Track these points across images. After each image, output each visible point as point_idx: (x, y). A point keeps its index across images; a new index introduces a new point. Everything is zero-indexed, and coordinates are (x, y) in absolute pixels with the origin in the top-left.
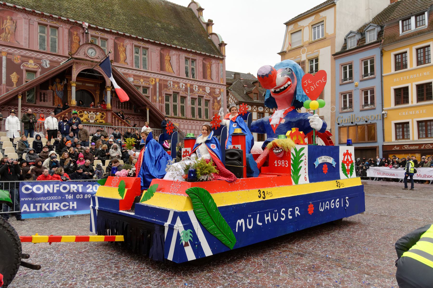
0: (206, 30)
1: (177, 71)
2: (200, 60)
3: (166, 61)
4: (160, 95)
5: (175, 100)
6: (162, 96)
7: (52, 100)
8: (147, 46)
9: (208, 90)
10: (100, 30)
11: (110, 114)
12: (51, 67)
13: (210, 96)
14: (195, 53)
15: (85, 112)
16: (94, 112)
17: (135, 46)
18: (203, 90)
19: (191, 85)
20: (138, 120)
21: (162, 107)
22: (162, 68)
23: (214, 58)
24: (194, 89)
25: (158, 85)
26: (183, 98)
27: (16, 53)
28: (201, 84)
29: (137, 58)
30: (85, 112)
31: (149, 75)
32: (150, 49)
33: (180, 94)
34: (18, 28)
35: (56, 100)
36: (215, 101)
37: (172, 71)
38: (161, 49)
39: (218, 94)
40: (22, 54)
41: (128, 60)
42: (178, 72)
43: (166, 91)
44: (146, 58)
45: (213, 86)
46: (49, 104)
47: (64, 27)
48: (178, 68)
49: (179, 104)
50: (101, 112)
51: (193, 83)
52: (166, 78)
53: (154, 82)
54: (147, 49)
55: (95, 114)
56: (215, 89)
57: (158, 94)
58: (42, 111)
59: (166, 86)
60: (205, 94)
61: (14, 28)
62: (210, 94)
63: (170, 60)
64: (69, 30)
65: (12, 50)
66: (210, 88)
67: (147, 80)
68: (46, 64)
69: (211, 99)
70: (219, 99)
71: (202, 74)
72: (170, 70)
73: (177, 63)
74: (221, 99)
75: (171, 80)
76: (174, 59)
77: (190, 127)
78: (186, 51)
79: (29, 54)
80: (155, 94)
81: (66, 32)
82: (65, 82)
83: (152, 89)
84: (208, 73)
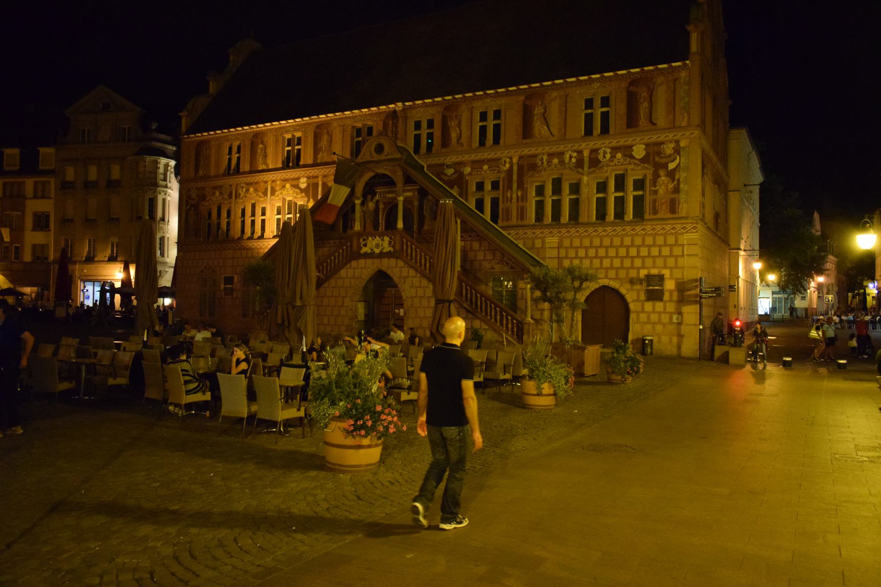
3: (535, 118)
4: (521, 186)
9: (639, 152)
13: (646, 165)
15: (370, 238)
16: (380, 237)
18: (624, 156)
19: (594, 151)
20: (479, 240)
24: (600, 157)
25: (515, 168)
29: (483, 130)
30: (370, 238)
39: (670, 155)
41: (464, 140)
42: (563, 130)
50: (388, 236)
53: (508, 166)
55: (381, 240)
57: (515, 185)
59: (533, 167)
60: (630, 164)
62: (644, 160)
63: (544, 114)
64: (384, 121)
66: (647, 145)
69: (649, 172)
70: (671, 166)
71: (625, 118)
72: (543, 132)
80: (510, 187)
83: (503, 178)
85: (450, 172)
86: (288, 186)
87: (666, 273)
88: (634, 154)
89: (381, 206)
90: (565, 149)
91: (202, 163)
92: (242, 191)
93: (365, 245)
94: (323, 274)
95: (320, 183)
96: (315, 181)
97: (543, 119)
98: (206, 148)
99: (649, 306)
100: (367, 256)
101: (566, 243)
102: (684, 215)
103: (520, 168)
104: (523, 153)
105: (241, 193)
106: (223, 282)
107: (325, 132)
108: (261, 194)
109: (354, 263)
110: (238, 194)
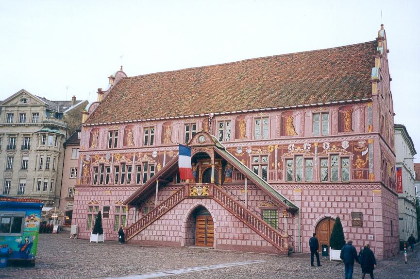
1: (301, 132)
2: (334, 111)
4: (279, 160)
6: (281, 163)
8: (267, 115)
9: (345, 145)
18: (337, 147)
21: (281, 173)
24: (324, 147)
25: (276, 151)
31: (267, 143)
32: (269, 117)
34: (173, 134)
38: (283, 113)
39: (363, 148)
41: (248, 135)
42: (303, 132)
43: (286, 156)
47: (199, 121)
48: (302, 127)
51: (323, 140)
53: (272, 150)
56: (357, 141)
57: (276, 161)
59: (286, 151)
65: (168, 149)
66: (350, 142)
69: (352, 156)
70: (364, 153)
71: (337, 126)
73: (301, 122)
74: (368, 153)
75: (292, 144)
77: (317, 192)
78: (311, 107)
81: (201, 124)
85: (240, 151)
86: (145, 156)
87: (363, 211)
88: (343, 146)
89: (200, 169)
91: (94, 140)
93: (192, 191)
95: (165, 155)
97: (291, 125)
99: (354, 230)
100: (193, 197)
101: (306, 192)
102: (371, 181)
106: (103, 209)
107: (168, 126)
108: (129, 159)
109: (186, 201)
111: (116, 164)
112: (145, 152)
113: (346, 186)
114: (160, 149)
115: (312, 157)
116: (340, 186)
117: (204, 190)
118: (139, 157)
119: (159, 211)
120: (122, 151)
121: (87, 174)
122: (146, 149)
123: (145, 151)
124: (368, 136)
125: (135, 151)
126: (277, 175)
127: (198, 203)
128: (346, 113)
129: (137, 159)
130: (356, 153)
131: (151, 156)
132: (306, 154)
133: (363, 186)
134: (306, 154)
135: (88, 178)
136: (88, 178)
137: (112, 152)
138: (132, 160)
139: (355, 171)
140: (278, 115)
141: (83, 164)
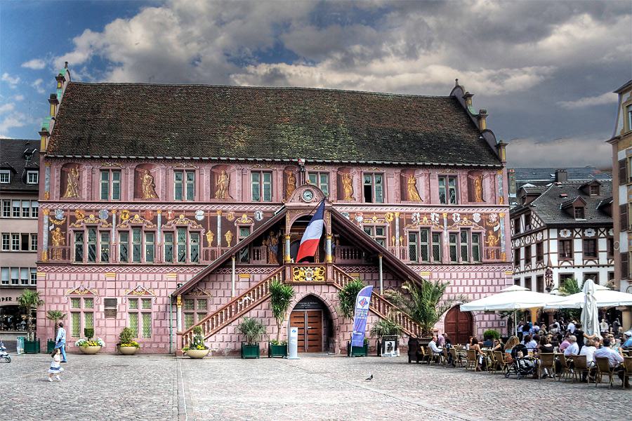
0: (477, 125)
1: (426, 197)
4: (402, 234)
5: (424, 239)
7: (266, 257)
8: (381, 170)
9: (477, 218)
10: (320, 163)
11: (330, 269)
12: (266, 219)
14: (455, 167)
16: (311, 268)
17: (365, 174)
21: (404, 250)
22: (403, 196)
23: (487, 168)
24: (454, 219)
25: (397, 220)
26: (437, 235)
27: (230, 209)
28: (466, 211)
31: (384, 209)
32: (385, 174)
33: (432, 230)
35: (270, 256)
36: (490, 232)
37: (418, 199)
40: (235, 209)
41: (356, 195)
43: (409, 228)
44: (380, 187)
45: (485, 211)
46: (263, 261)
48: (428, 192)
49: (430, 244)
51: (452, 211)
52: (409, 210)
53: (392, 219)
54: (382, 174)
56: (489, 214)
57: (397, 234)
58: (256, 270)
59: (410, 221)
61: (228, 182)
62: (480, 223)
65: (226, 208)
66: (481, 214)
67: (384, 216)
68: (259, 216)
69: (484, 231)
73: (426, 185)
76: (422, 181)
78: (439, 167)
79: (242, 208)
80: (394, 234)
81: (280, 173)
82: (280, 234)
84: (477, 193)
86: (182, 216)
90: (431, 211)
92: (125, 217)
93: (297, 274)
94: (254, 298)
95: (219, 217)
96: (213, 214)
97: (414, 188)
98: (75, 171)
102: (504, 260)
103: (401, 221)
104: (402, 211)
105: (123, 218)
107: (223, 172)
108: (149, 221)
110: (120, 220)
111: (123, 227)
112: (182, 211)
113: (479, 267)
114: (210, 207)
115: (441, 231)
116: (473, 267)
117: (317, 273)
118: (170, 218)
119: (241, 305)
120: (133, 207)
121: (61, 244)
122: (182, 207)
123: (180, 209)
124: (499, 209)
125: (160, 207)
126: (399, 253)
127: (308, 293)
128: (476, 180)
129: (164, 221)
130: (489, 228)
131: (193, 218)
132: (433, 226)
133: (496, 267)
134: (433, 226)
135: (64, 250)
136: (64, 250)
137: (111, 207)
138: (154, 221)
139: (488, 250)
140: (396, 173)
141: (50, 224)
